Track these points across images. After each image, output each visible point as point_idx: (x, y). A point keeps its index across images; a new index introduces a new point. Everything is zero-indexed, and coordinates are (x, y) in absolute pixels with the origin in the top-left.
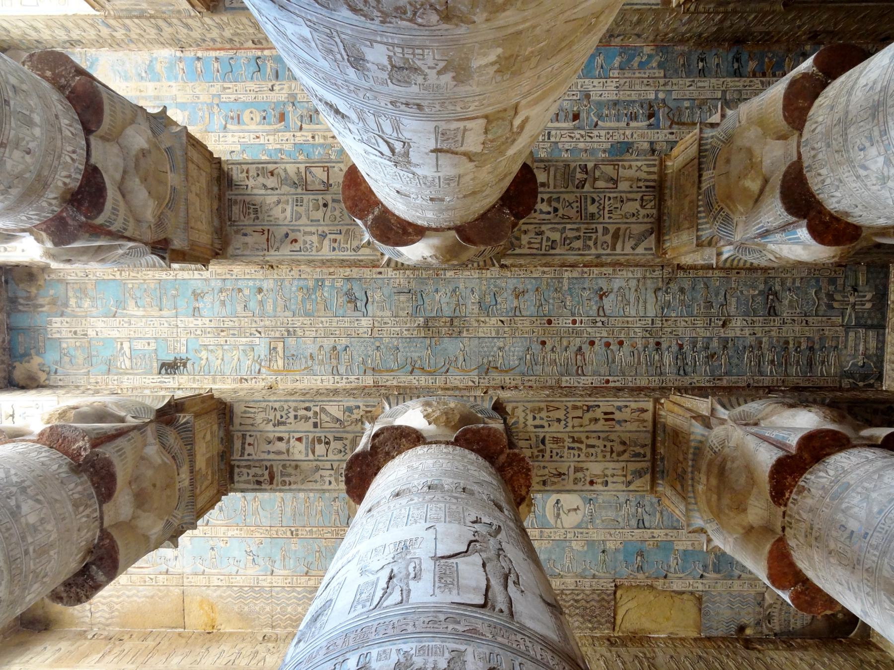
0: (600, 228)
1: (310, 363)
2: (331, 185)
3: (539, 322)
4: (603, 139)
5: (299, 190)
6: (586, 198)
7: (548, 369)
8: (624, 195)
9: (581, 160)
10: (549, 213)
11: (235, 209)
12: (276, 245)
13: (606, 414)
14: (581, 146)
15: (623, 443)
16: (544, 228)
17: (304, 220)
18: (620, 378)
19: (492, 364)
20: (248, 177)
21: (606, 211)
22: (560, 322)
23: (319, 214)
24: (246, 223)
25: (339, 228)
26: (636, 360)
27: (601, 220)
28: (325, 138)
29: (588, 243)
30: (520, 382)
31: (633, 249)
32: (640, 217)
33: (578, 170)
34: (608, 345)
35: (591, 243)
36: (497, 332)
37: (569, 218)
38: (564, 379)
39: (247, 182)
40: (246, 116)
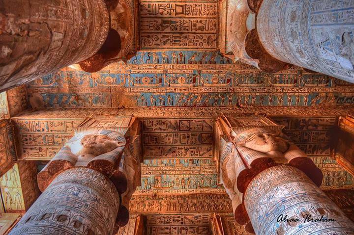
1: (172, 185)
2: (191, 128)
4: (306, 91)
5: (176, 131)
6: (303, 133)
8: (320, 132)
11: (147, 138)
12: (166, 153)
14: (297, 94)
17: (179, 143)
20: (152, 125)
23: (185, 141)
24: (152, 144)
25: (194, 146)
28: (180, 90)
31: (321, 153)
39: (152, 127)
40: (143, 79)
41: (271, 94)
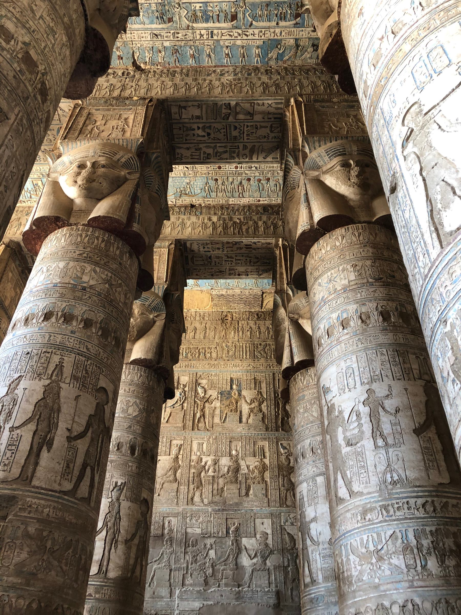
0: (241, 146)
3: (212, 168)
6: (230, 126)
7: (220, 194)
9: (226, 100)
10: (204, 136)
13: (246, 245)
15: (257, 258)
16: (201, 146)
18: (267, 199)
19: (183, 192)
21: (245, 135)
22: (227, 167)
26: (278, 189)
27: (242, 140)
29: (233, 155)
30: (202, 202)
32: (270, 138)
33: (224, 107)
34: (259, 181)
35: (235, 155)
36: (185, 174)
37: (219, 139)
38: (231, 200)
41: (191, 43)
